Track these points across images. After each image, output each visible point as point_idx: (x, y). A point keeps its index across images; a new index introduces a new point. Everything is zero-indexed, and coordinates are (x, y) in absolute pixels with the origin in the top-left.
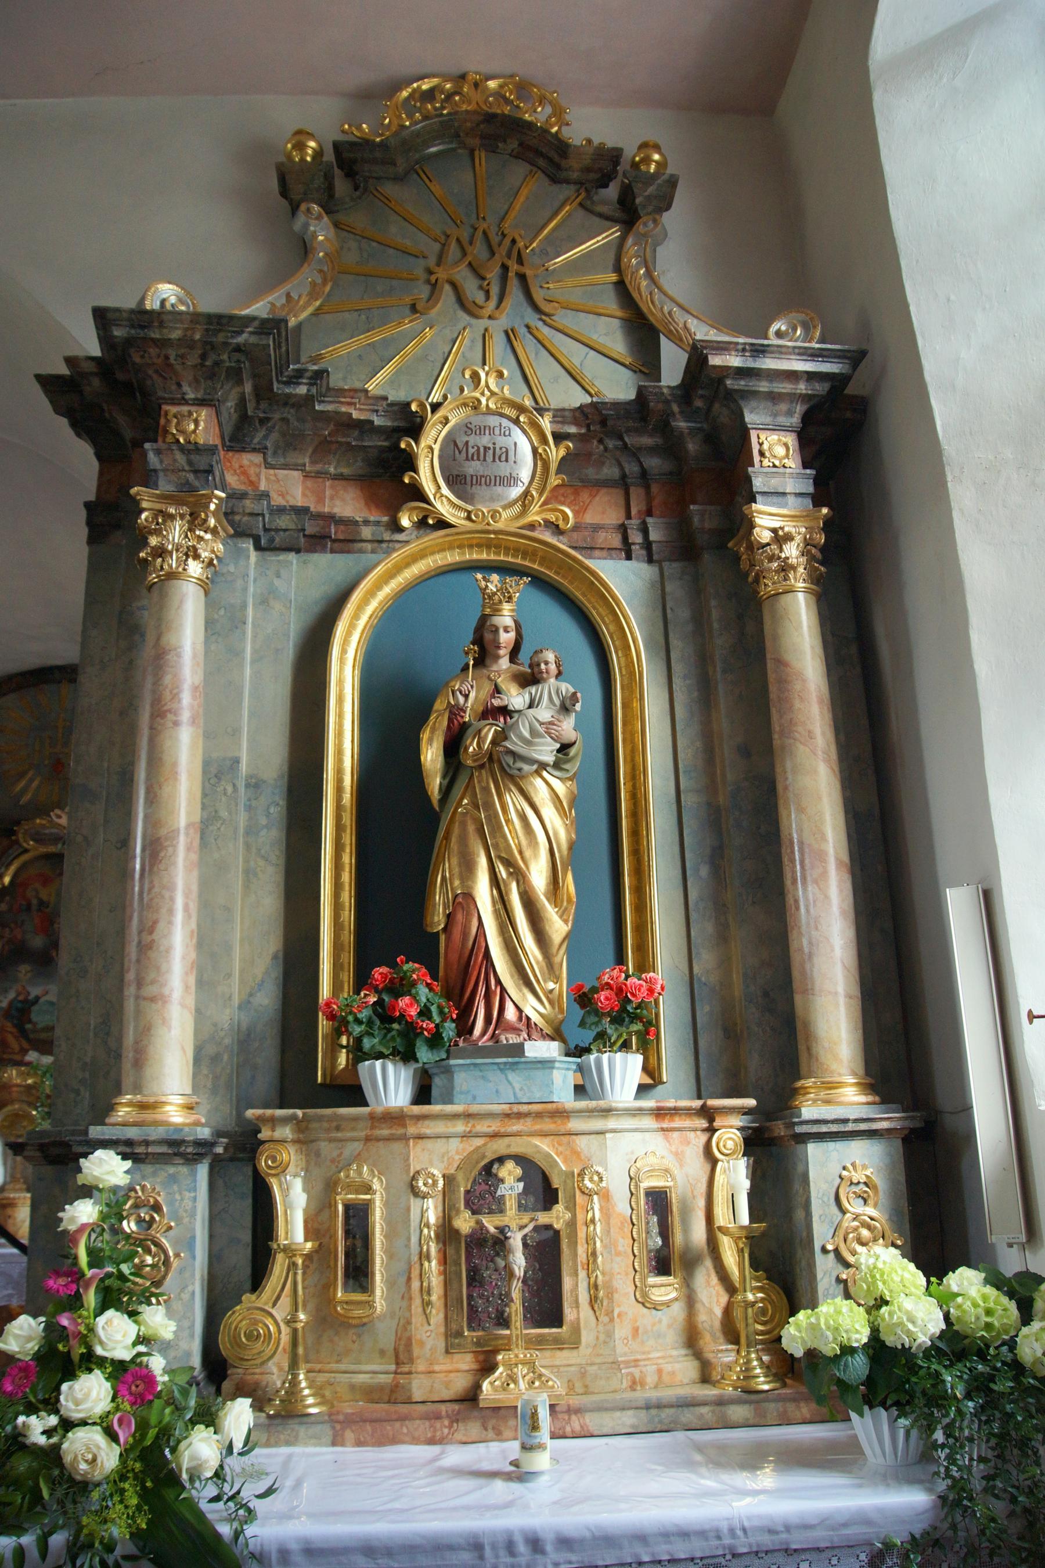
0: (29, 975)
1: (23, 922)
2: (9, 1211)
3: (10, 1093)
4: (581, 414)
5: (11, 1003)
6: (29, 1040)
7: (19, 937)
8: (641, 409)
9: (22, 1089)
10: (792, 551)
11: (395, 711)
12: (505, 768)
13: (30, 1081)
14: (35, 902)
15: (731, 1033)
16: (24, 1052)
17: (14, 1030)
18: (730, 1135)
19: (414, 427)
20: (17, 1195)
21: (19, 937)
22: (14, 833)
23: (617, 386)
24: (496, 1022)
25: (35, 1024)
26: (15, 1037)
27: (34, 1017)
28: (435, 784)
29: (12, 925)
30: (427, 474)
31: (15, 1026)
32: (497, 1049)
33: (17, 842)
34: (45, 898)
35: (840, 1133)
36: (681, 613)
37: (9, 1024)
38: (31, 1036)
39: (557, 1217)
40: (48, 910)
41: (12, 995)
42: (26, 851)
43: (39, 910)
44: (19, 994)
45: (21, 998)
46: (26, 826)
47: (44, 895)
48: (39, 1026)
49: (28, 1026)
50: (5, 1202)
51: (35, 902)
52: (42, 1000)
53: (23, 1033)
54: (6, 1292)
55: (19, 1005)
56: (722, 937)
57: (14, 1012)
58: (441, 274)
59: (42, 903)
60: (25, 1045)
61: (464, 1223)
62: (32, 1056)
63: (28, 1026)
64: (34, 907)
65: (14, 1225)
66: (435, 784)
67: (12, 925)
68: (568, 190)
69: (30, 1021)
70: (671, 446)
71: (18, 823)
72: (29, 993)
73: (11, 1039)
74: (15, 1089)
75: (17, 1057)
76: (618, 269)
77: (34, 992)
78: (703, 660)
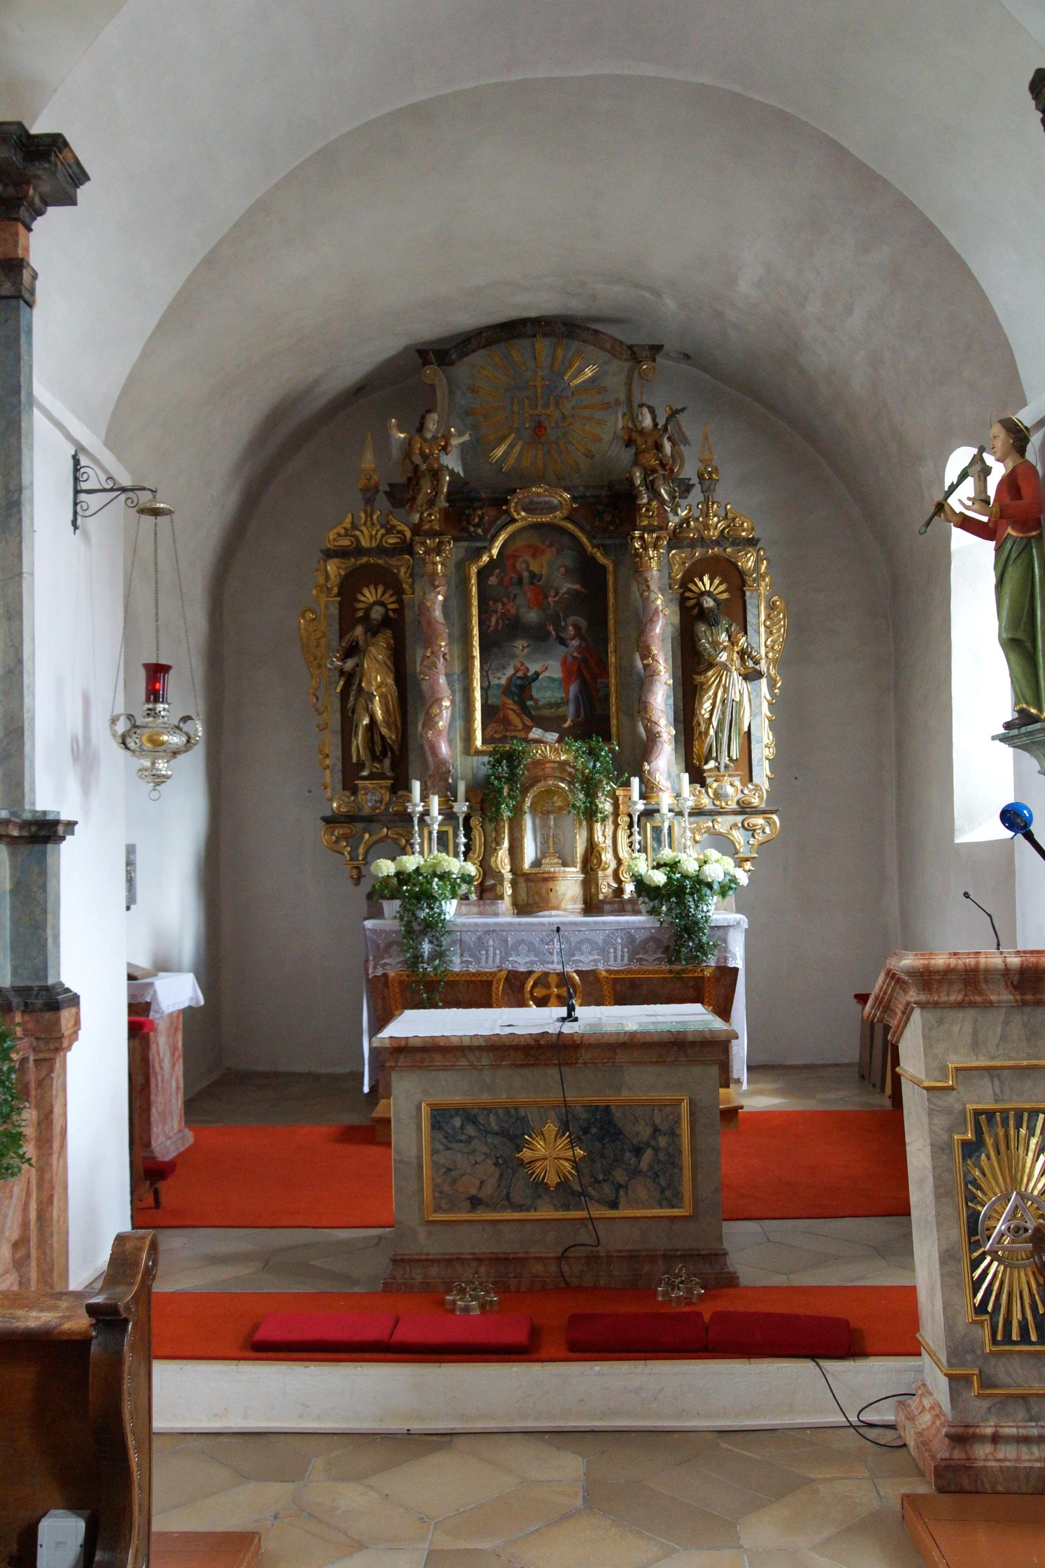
0: (526, 651)
1: (515, 595)
2: (551, 885)
3: (543, 769)
5: (510, 679)
6: (532, 718)
7: (513, 611)
9: (556, 765)
13: (563, 758)
14: (526, 574)
16: (530, 729)
17: (515, 707)
20: (557, 869)
21: (513, 611)
22: (506, 502)
25: (536, 701)
26: (518, 715)
27: (534, 693)
29: (505, 600)
31: (515, 702)
33: (507, 512)
34: (536, 570)
37: (510, 701)
38: (533, 712)
40: (541, 583)
41: (510, 672)
42: (514, 521)
43: (531, 583)
44: (517, 671)
45: (520, 674)
46: (520, 494)
47: (534, 567)
48: (540, 703)
49: (530, 703)
50: (546, 875)
51: (526, 574)
52: (541, 677)
53: (525, 710)
54: (592, 958)
55: (519, 682)
57: (513, 689)
59: (533, 575)
60: (529, 723)
62: (536, 733)
63: (530, 703)
64: (526, 580)
65: (557, 897)
67: (505, 600)
69: (531, 698)
71: (513, 491)
72: (528, 670)
73: (512, 716)
74: (548, 765)
75: (520, 735)
77: (533, 668)
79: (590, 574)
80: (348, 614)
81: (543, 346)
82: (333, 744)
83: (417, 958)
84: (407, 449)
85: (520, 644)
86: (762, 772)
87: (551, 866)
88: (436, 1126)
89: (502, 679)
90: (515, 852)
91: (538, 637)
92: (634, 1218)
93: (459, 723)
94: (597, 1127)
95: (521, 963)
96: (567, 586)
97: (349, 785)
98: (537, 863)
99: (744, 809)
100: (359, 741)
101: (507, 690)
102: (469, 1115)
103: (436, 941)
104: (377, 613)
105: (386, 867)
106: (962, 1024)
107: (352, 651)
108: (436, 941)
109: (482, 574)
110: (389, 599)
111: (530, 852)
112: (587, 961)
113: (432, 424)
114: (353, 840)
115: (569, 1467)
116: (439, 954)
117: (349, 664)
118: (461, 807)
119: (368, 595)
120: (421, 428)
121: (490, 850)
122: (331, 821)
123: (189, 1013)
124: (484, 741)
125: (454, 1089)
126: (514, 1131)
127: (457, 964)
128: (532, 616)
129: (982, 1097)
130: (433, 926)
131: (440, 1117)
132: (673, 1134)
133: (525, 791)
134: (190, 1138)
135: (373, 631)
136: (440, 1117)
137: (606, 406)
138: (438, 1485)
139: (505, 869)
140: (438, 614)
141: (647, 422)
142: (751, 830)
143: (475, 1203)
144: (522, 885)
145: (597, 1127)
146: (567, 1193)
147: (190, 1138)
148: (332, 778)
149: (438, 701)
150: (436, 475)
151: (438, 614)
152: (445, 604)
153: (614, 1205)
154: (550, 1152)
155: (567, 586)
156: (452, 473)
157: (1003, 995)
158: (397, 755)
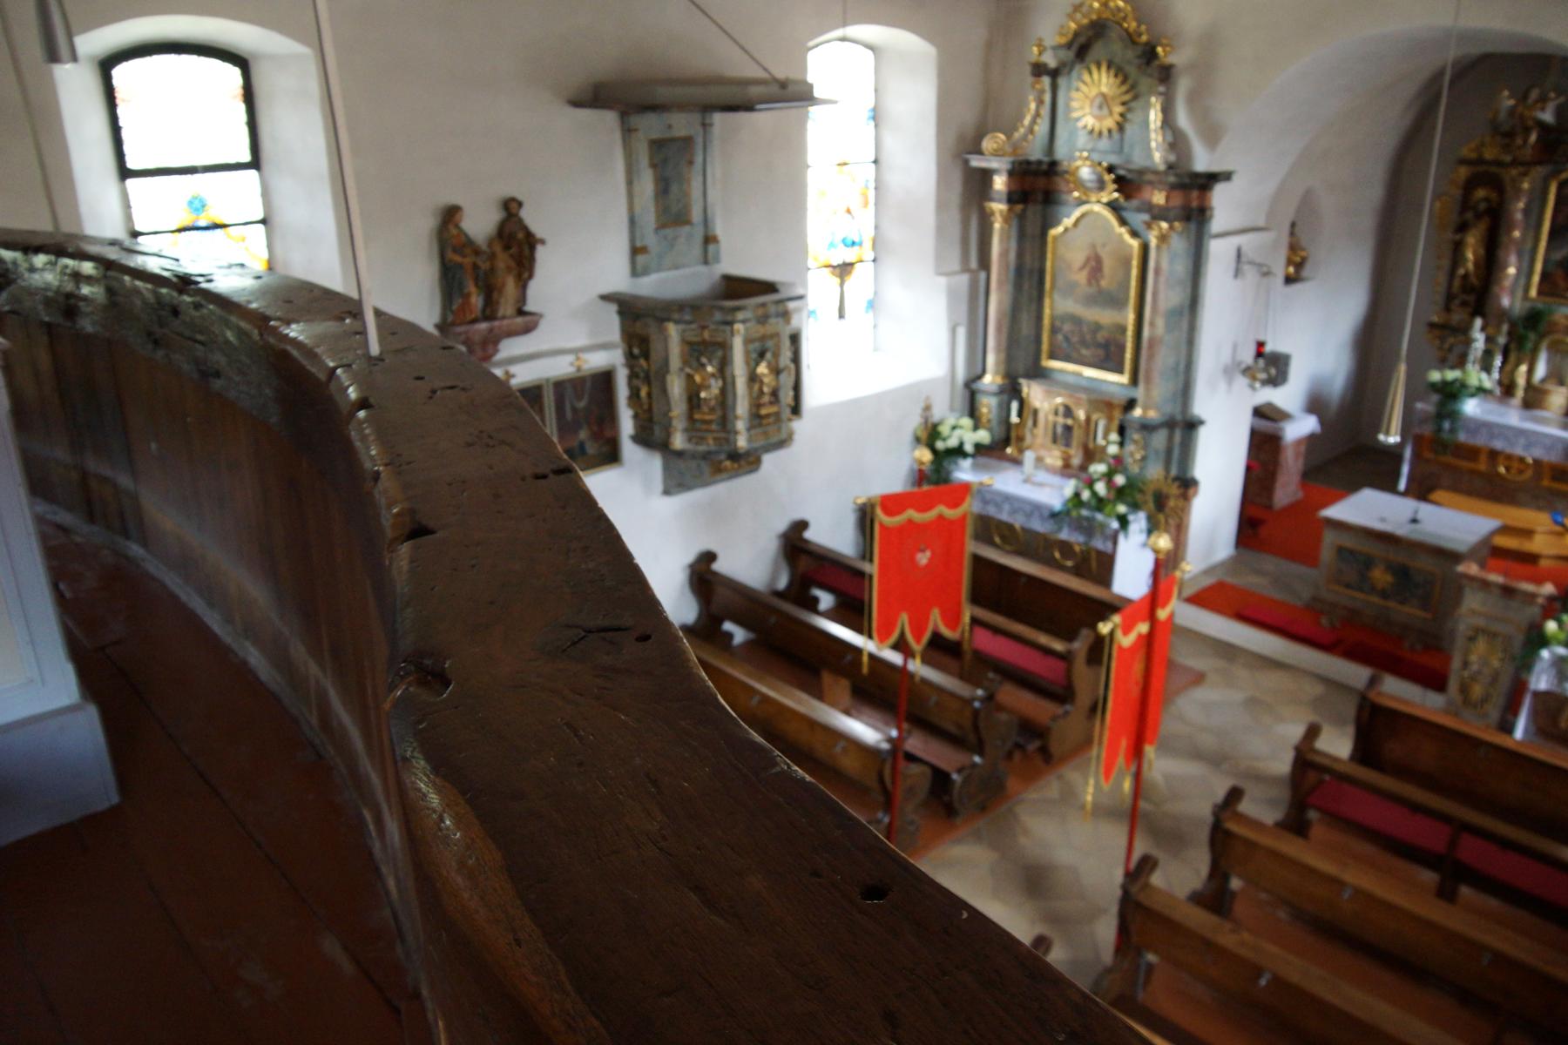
80: (1466, 204)
82: (1442, 279)
83: (1440, 429)
84: (1512, 112)
87: (1549, 386)
89: (1558, 256)
90: (1530, 371)
92: (1409, 612)
93: (1522, 281)
94: (1402, 574)
95: (1498, 445)
97: (1447, 309)
98: (1543, 381)
100: (1457, 283)
102: (1351, 552)
103: (1453, 422)
104: (1483, 206)
105: (1435, 376)
106: (1480, 596)
107: (1462, 228)
108: (1453, 422)
110: (1494, 196)
111: (1541, 370)
112: (1538, 453)
113: (1534, 94)
114: (1442, 339)
115: (1319, 689)
116: (1453, 430)
117: (1458, 237)
118: (1502, 340)
119: (1481, 193)
120: (1525, 97)
121: (1517, 365)
122: (1432, 326)
123: (1311, 439)
124: (1540, 292)
125: (1348, 542)
126: (1368, 563)
127: (1462, 437)
129: (1481, 622)
130: (1454, 416)
131: (1341, 550)
133: (1542, 336)
134: (1300, 495)
135: (1478, 216)
136: (1341, 550)
138: (1273, 679)
139: (1521, 381)
140: (1519, 216)
143: (1348, 586)
145: (1402, 574)
146: (1384, 594)
147: (1300, 495)
148: (1440, 299)
149: (1506, 267)
151: (1519, 216)
152: (1526, 211)
153: (1402, 603)
154: (1380, 576)
156: (1541, 125)
158: (1475, 295)
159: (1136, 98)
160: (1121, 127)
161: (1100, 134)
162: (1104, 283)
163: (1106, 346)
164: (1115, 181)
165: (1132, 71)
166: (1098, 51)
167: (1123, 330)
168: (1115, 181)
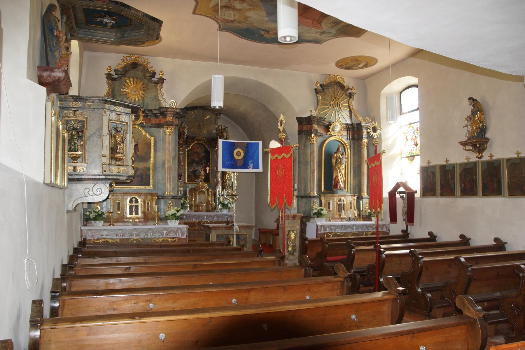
4: (346, 124)
8: (352, 125)
10: (365, 144)
11: (329, 156)
12: (341, 163)
15: (354, 189)
18: (355, 198)
19: (331, 125)
23: (349, 122)
24: (340, 187)
28: (334, 165)
30: (331, 130)
32: (341, 189)
35: (365, 198)
36: (352, 146)
39: (345, 203)
56: (354, 179)
58: (332, 103)
59: (197, 152)
61: (339, 203)
66: (334, 165)
68: (343, 92)
70: (353, 127)
76: (348, 103)
77: (197, 168)
78: (354, 151)
79: (207, 153)
81: (201, 111)
85: (194, 164)
86: (235, 188)
88: (217, 237)
91: (198, 163)
96: (203, 154)
99: (232, 195)
101: (192, 172)
109: (188, 151)
125: (220, 232)
128: (197, 159)
132: (247, 238)
137: (211, 123)
141: (220, 128)
142: (233, 199)
144: (196, 207)
150: (184, 134)
155: (203, 154)
157: (291, 218)
159: (147, 89)
160: (143, 99)
161: (135, 100)
162: (138, 153)
163: (142, 175)
164: (144, 116)
165: (146, 81)
166: (132, 73)
167: (149, 169)
168: (144, 116)
